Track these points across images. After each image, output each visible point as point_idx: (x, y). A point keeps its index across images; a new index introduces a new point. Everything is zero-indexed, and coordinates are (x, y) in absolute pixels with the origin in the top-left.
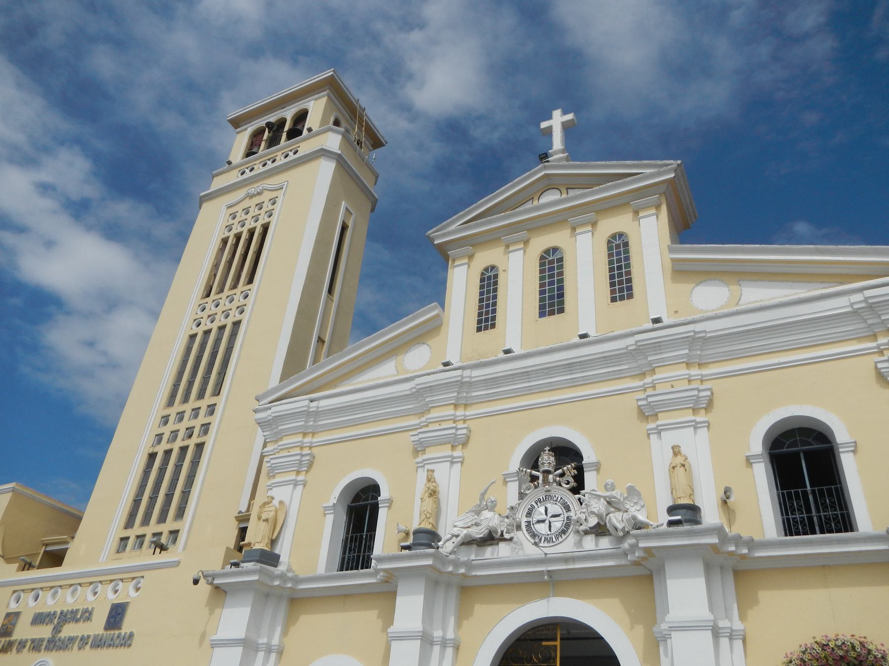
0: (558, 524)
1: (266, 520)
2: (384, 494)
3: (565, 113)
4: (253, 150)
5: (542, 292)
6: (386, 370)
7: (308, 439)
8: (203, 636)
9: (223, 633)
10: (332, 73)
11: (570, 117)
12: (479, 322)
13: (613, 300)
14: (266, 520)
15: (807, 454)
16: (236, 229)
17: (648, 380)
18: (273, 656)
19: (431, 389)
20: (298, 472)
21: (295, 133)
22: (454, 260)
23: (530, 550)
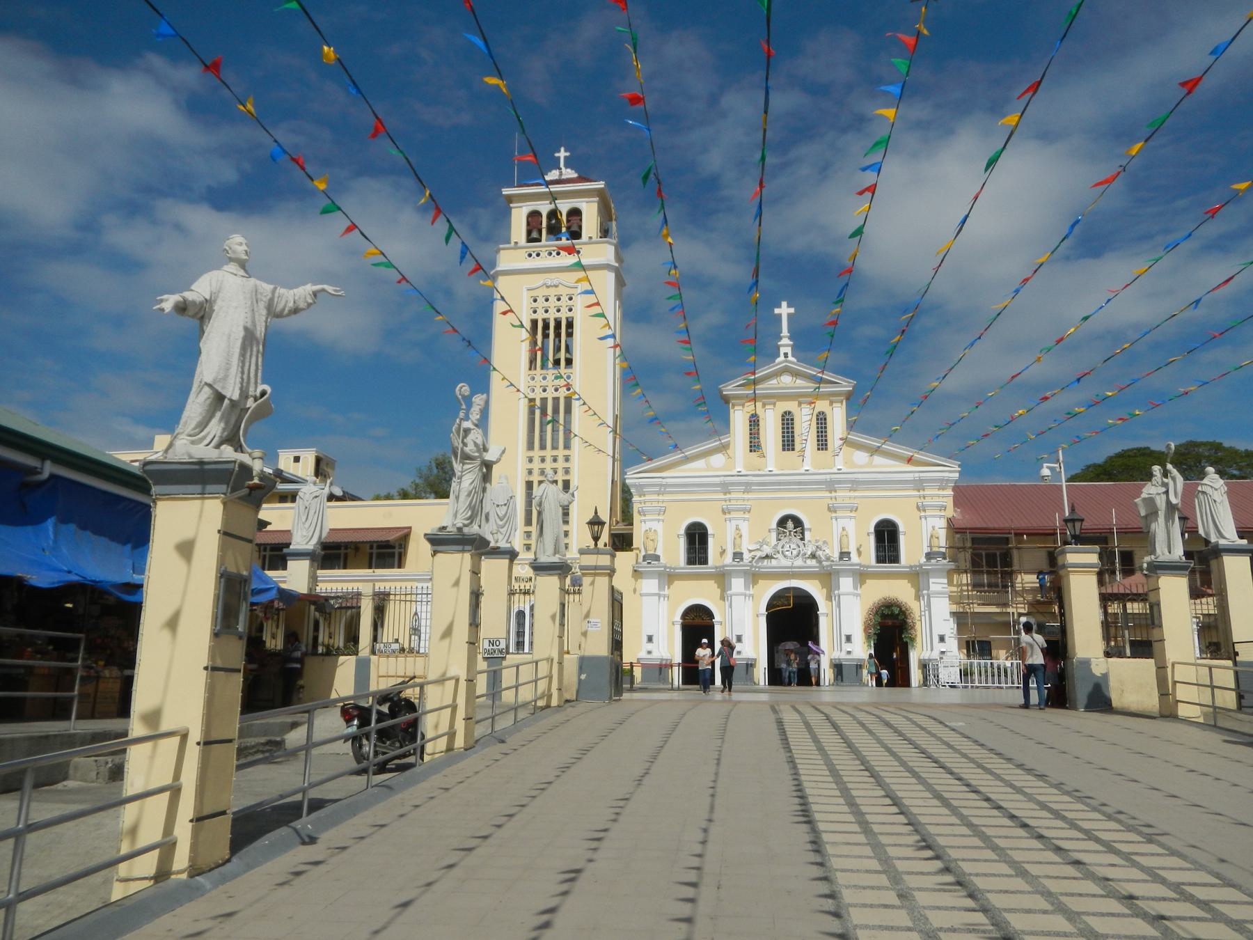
0: (795, 552)
1: (652, 540)
2: (710, 532)
3: (789, 306)
4: (535, 235)
5: (783, 437)
6: (700, 463)
7: (661, 497)
8: (635, 591)
9: (644, 591)
10: (603, 186)
11: (792, 310)
12: (751, 446)
13: (818, 449)
14: (652, 540)
15: (888, 531)
16: (540, 316)
17: (833, 494)
18: (666, 599)
19: (733, 484)
20: (659, 514)
21: (576, 234)
22: (733, 405)
23: (785, 562)
